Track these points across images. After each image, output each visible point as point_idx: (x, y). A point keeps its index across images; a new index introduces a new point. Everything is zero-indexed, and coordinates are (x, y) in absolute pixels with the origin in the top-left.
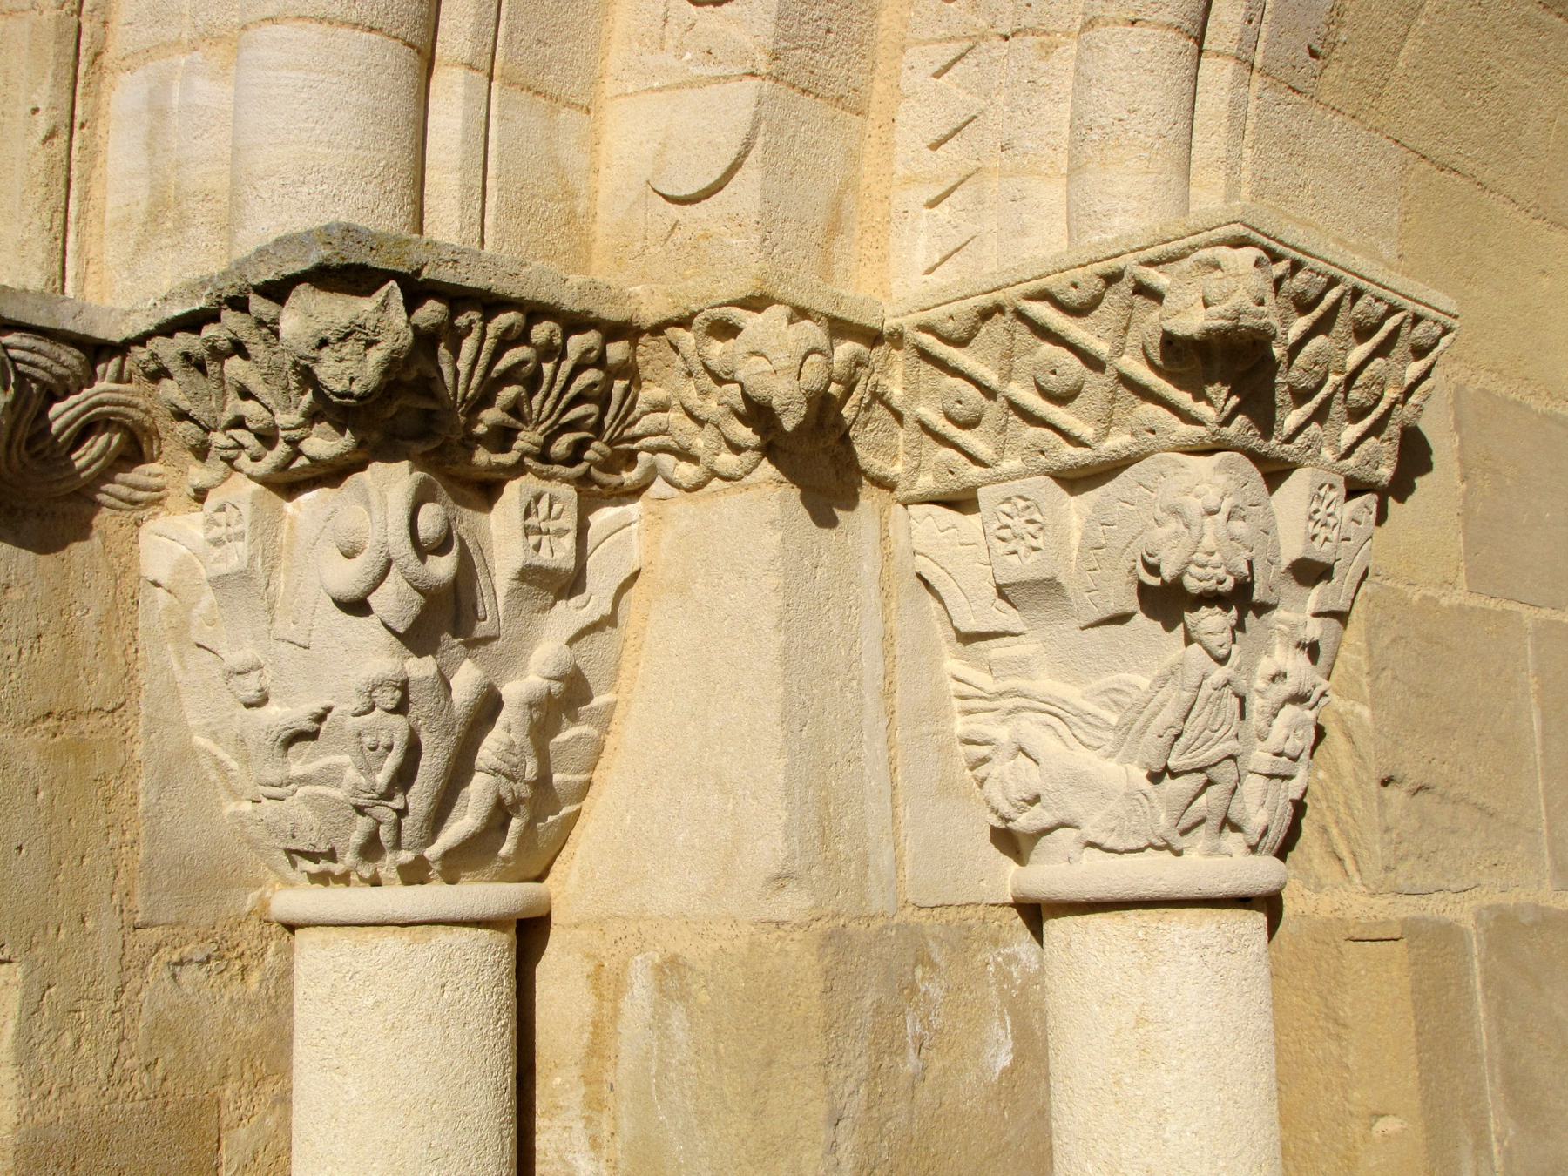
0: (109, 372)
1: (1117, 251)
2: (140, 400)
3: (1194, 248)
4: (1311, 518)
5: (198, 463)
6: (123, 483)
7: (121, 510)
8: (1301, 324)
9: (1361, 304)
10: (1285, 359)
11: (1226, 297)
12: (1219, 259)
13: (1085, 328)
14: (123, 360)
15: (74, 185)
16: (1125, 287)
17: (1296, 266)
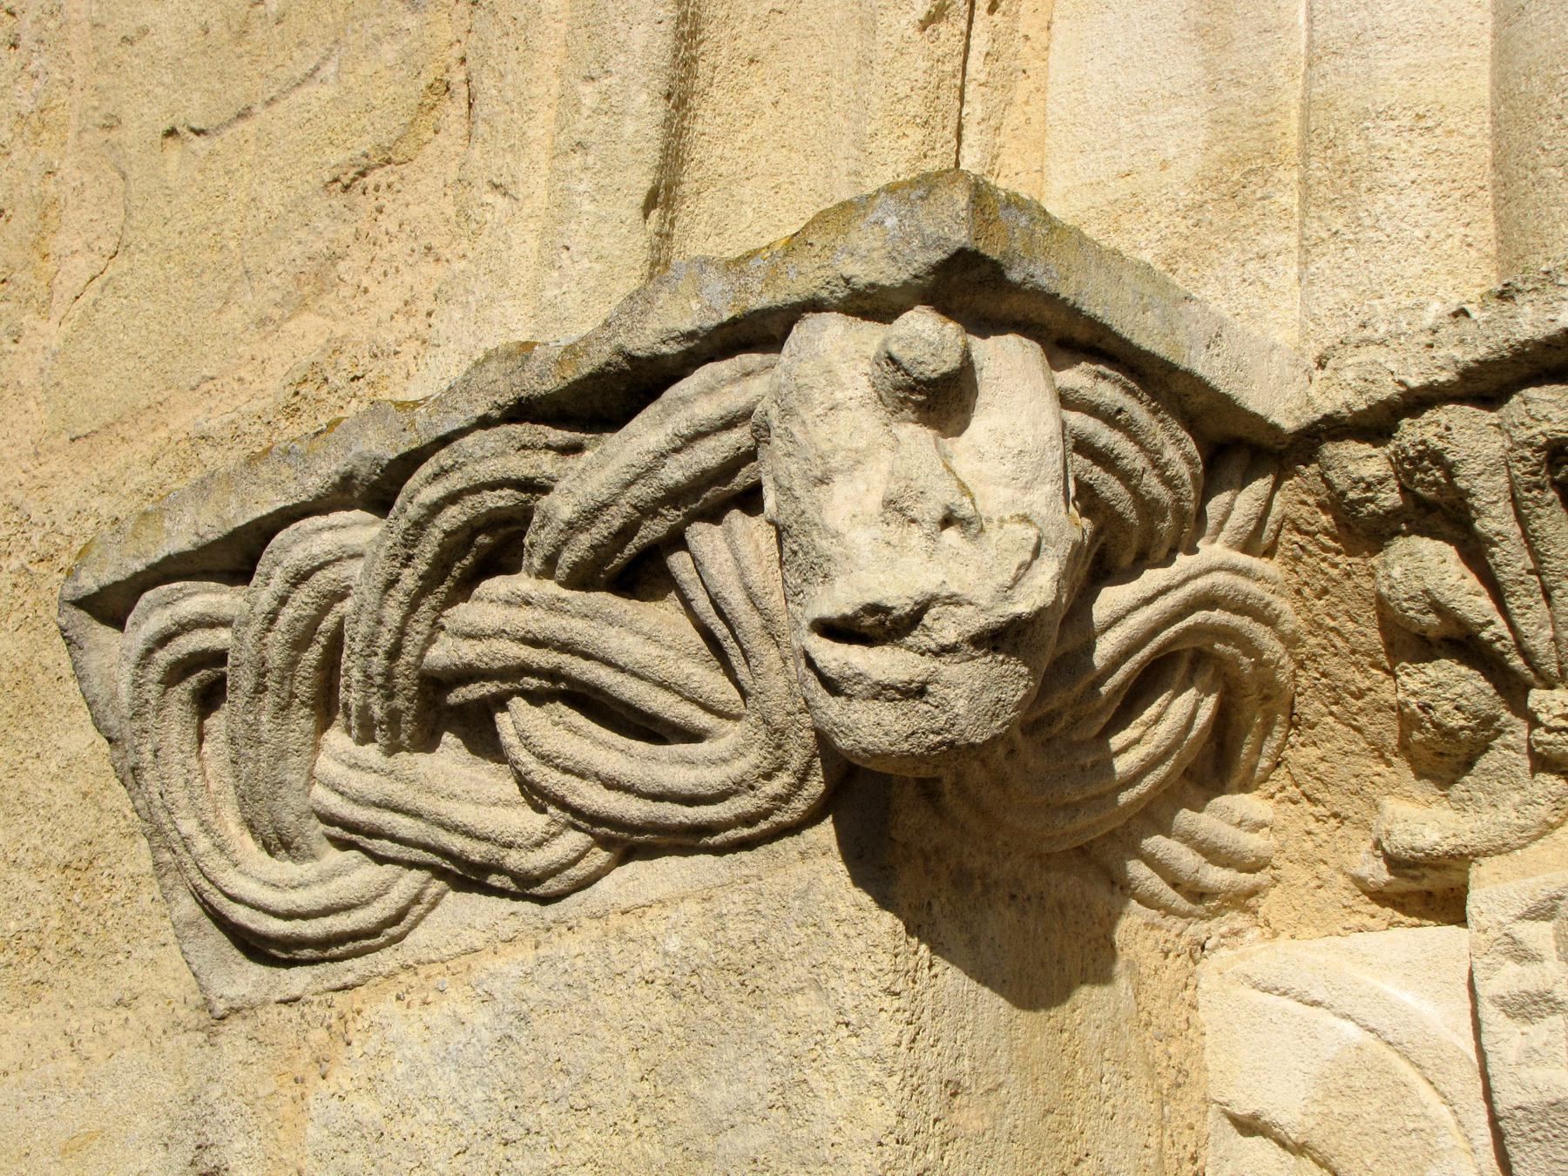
0: (1236, 519)
2: (1282, 605)
5: (1427, 789)
6: (1188, 839)
7: (1168, 911)
14: (1276, 486)
15: (970, 135)
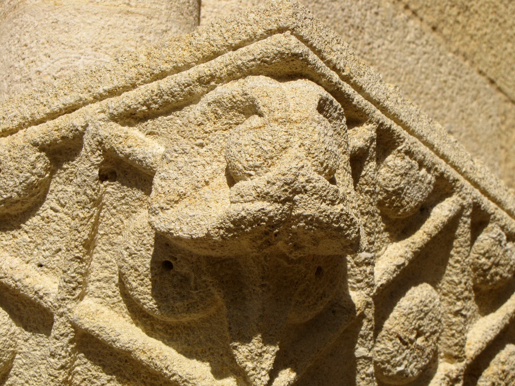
1: (70, 100)
3: (207, 82)
8: (391, 256)
9: (485, 239)
10: (370, 313)
11: (269, 161)
12: (252, 94)
13: (16, 252)
16: (86, 165)
17: (385, 142)
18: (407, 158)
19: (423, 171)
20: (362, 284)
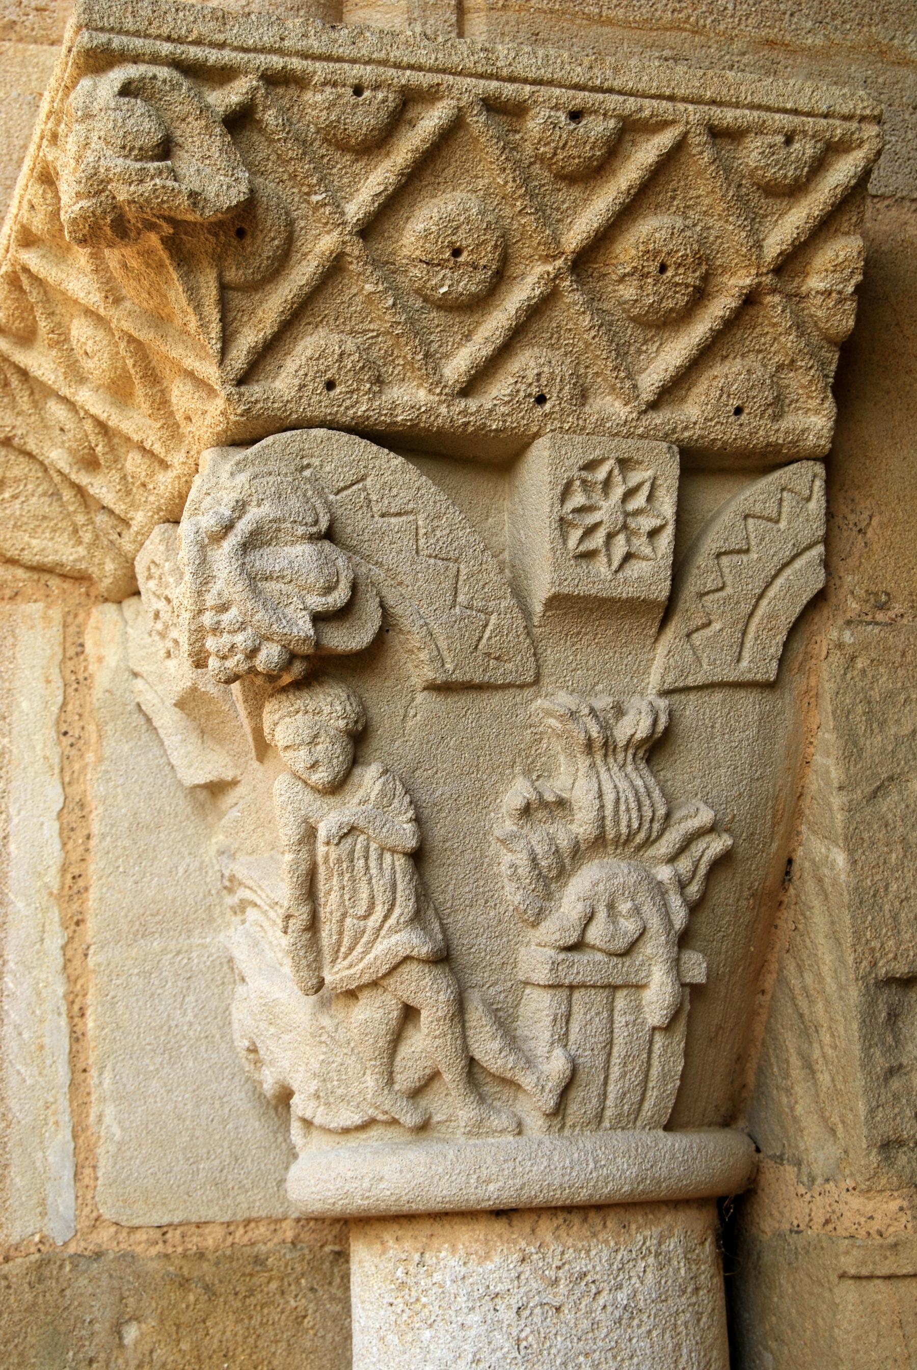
4: (563, 524)
18: (328, 89)
19: (367, 94)
20: (329, 226)
